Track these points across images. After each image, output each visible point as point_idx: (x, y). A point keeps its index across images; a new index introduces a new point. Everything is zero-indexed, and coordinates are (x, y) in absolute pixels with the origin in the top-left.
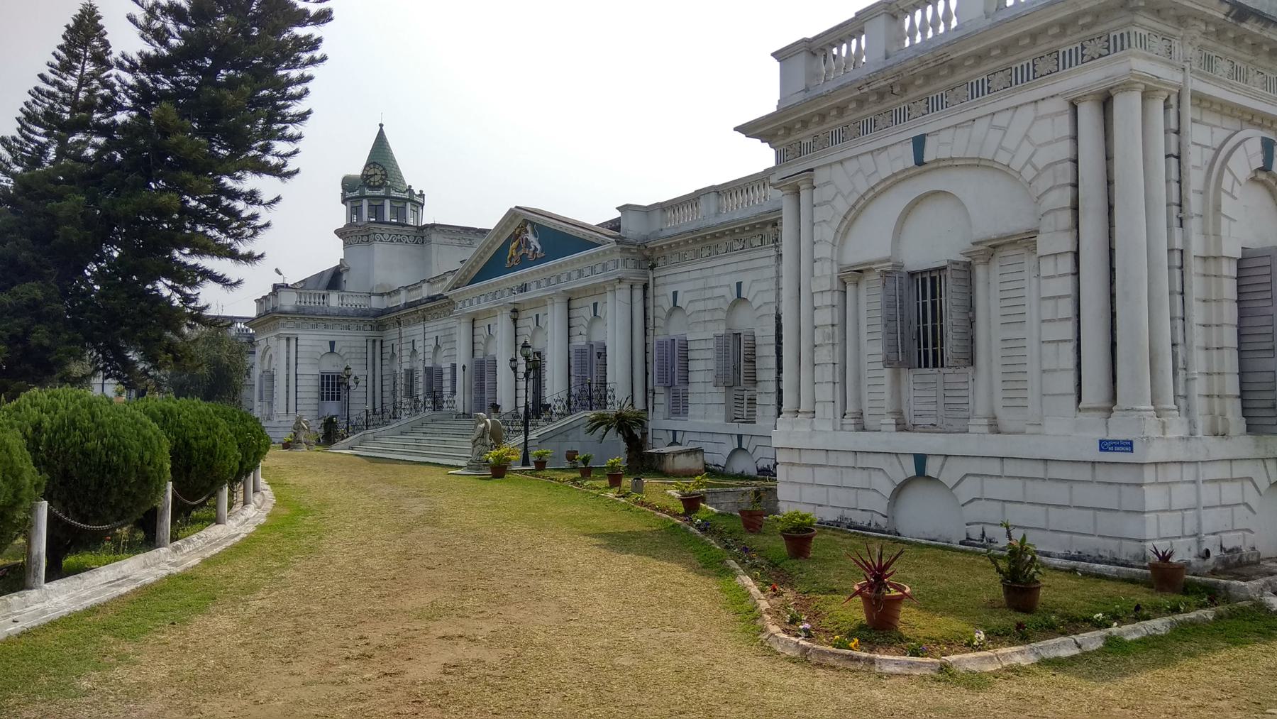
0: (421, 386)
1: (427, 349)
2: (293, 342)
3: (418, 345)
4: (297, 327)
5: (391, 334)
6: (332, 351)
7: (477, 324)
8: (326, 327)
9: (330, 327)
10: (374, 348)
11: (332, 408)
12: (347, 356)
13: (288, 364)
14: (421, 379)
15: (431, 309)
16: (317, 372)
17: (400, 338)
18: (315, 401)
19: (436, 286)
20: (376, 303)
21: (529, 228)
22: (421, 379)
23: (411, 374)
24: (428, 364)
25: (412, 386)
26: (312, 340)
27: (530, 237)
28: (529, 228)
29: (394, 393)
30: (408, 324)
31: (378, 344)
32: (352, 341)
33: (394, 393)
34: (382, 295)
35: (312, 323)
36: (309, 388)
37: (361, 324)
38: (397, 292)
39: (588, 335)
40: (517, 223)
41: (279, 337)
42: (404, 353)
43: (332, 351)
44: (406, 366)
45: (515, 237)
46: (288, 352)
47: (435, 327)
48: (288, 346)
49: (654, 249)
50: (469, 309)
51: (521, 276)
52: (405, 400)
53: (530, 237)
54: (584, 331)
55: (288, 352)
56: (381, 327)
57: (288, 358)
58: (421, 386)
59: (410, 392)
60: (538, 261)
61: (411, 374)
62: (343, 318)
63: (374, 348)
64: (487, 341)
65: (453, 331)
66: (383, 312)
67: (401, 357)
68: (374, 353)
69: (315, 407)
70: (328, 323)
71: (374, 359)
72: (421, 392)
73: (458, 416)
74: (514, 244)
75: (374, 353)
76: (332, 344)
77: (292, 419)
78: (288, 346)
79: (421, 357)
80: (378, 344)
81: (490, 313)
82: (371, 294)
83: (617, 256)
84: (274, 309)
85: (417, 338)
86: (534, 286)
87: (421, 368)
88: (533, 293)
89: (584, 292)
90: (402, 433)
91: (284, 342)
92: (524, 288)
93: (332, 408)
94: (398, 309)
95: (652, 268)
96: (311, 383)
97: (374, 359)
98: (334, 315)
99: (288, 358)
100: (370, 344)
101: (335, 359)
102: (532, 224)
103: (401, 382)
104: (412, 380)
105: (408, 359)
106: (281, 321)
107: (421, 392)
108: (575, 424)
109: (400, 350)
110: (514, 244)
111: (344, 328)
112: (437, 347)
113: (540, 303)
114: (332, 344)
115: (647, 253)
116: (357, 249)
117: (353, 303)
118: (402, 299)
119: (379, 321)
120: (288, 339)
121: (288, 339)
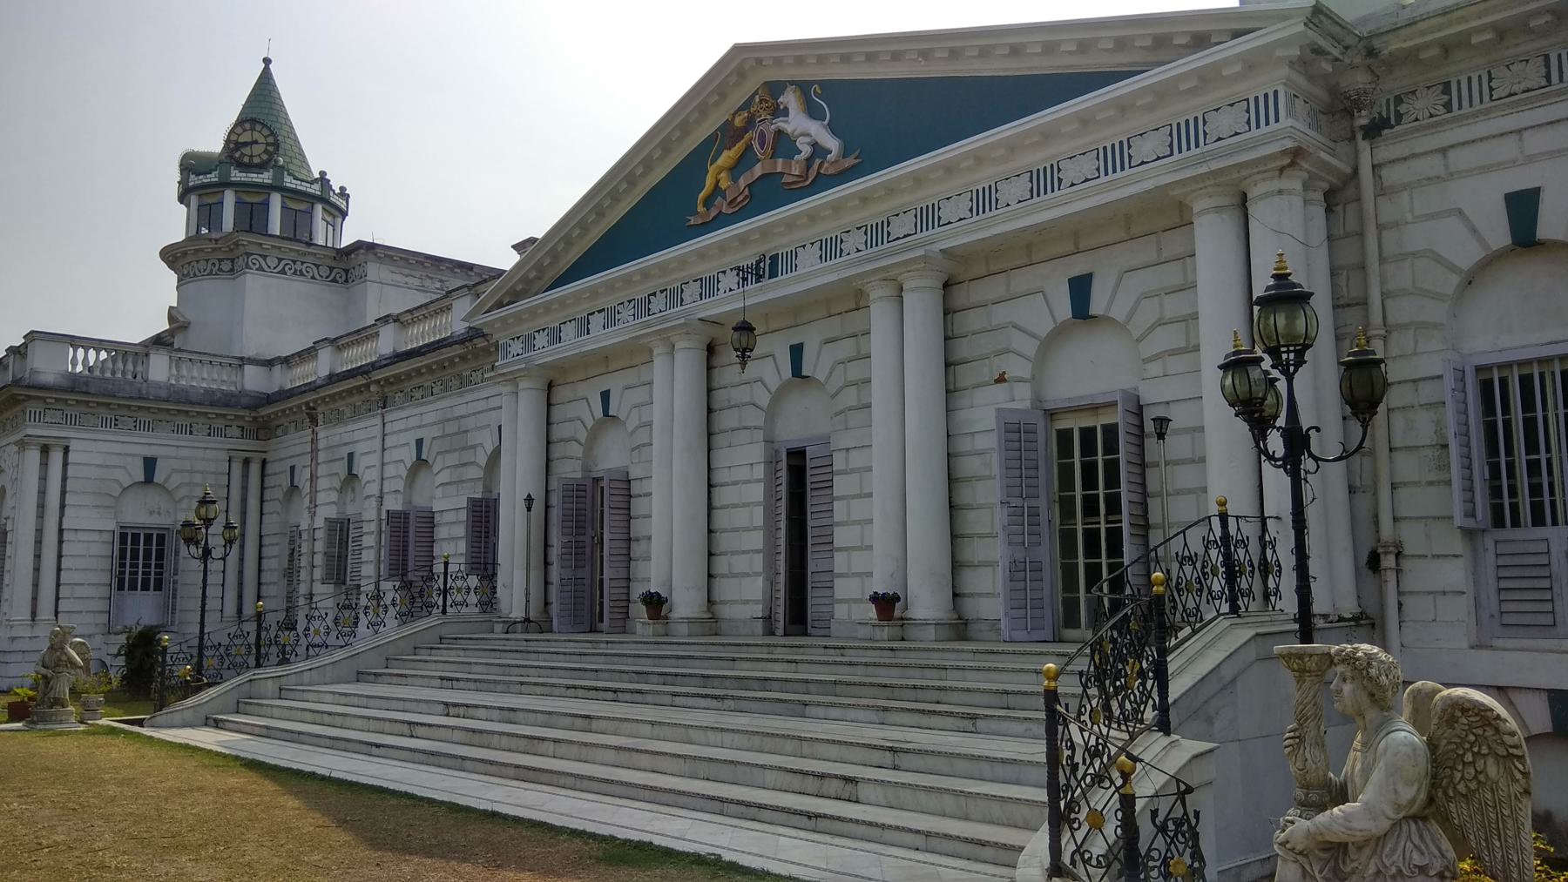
0: (368, 555)
1: (390, 471)
2: (56, 458)
3: (367, 467)
4: (71, 421)
5: (291, 446)
6: (149, 479)
7: (561, 394)
8: (138, 425)
9: (147, 427)
10: (245, 476)
11: (142, 609)
12: (183, 492)
13: (41, 507)
14: (369, 541)
15: (409, 376)
16: (111, 525)
17: (314, 451)
18: (104, 591)
19: (415, 330)
20: (254, 380)
21: (790, 99)
22: (369, 541)
23: (341, 532)
24: (394, 504)
25: (342, 557)
26: (103, 455)
27: (797, 122)
28: (790, 99)
29: (291, 573)
30: (340, 419)
31: (255, 469)
32: (196, 462)
33: (291, 573)
34: (269, 364)
35: (103, 412)
36: (88, 559)
37: (220, 423)
38: (308, 354)
39: (1036, 380)
40: (738, 98)
41: (22, 445)
42: (323, 483)
43: (149, 479)
44: (326, 512)
45: (728, 134)
46: (43, 479)
47: (413, 421)
48: (44, 464)
49: (1394, 62)
50: (546, 353)
51: (765, 232)
52: (319, 588)
53: (797, 122)
54: (1017, 368)
55: (43, 479)
56: (264, 429)
57: (42, 493)
58: (368, 555)
59: (338, 570)
60: (823, 182)
61: (341, 532)
62: (176, 408)
63: (245, 476)
64: (595, 433)
65: (470, 423)
66: (269, 399)
67: (314, 492)
68: (245, 488)
69: (103, 606)
70: (144, 417)
71: (244, 500)
72: (368, 570)
73: (510, 626)
74: (727, 157)
75: (245, 488)
76: (150, 464)
77: (43, 632)
78: (44, 464)
79: (373, 489)
80: (255, 469)
81: (633, 355)
82: (243, 361)
83: (1274, 80)
84: (16, 382)
85: (360, 449)
86: (809, 260)
87: (370, 512)
88: (810, 274)
89: (1022, 251)
90: (360, 677)
91: (33, 456)
92: (765, 268)
93: (142, 609)
94: (312, 388)
95: (1374, 130)
96: (96, 549)
97: (244, 500)
98: (158, 399)
99: (42, 493)
100: (237, 470)
101: (152, 497)
102: (803, 87)
103: (316, 551)
104: (344, 543)
105: (334, 496)
106: (32, 407)
107: (368, 570)
108: (1228, 673)
109: (313, 478)
110: (727, 157)
111: (179, 429)
112: (421, 463)
113: (849, 300)
114: (150, 464)
115: (1358, 80)
116: (212, 290)
117: (200, 379)
118: (324, 365)
119: (260, 418)
120: (45, 450)
121: (45, 450)
